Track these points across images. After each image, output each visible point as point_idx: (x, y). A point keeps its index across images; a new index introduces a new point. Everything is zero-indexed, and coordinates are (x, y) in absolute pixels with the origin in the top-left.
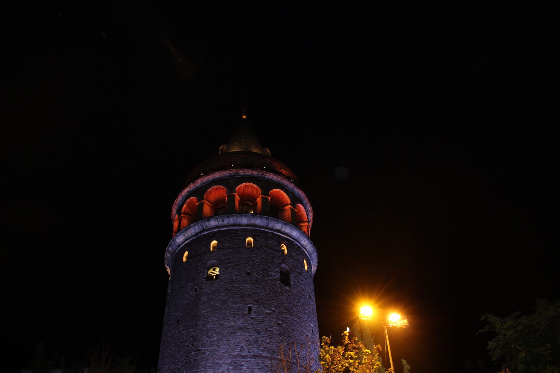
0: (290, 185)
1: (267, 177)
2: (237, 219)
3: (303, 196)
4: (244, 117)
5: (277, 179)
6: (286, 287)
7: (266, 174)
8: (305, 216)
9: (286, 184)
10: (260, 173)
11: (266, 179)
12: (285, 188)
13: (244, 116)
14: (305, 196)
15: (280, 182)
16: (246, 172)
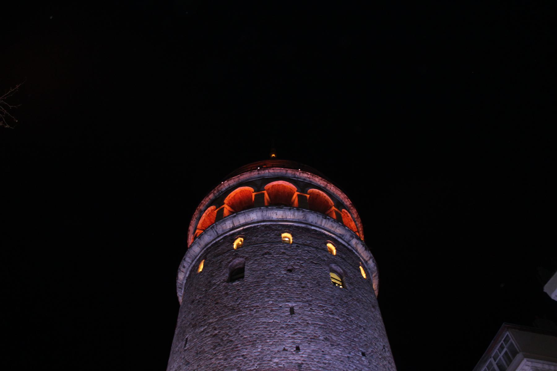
0: (253, 174)
1: (224, 189)
2: (190, 254)
3: (278, 171)
4: (274, 155)
5: (234, 182)
6: (234, 284)
7: (221, 187)
8: (292, 187)
9: (248, 178)
10: (215, 192)
11: (224, 192)
12: (249, 182)
13: (273, 154)
14: (282, 169)
15: (240, 181)
16: (205, 203)
